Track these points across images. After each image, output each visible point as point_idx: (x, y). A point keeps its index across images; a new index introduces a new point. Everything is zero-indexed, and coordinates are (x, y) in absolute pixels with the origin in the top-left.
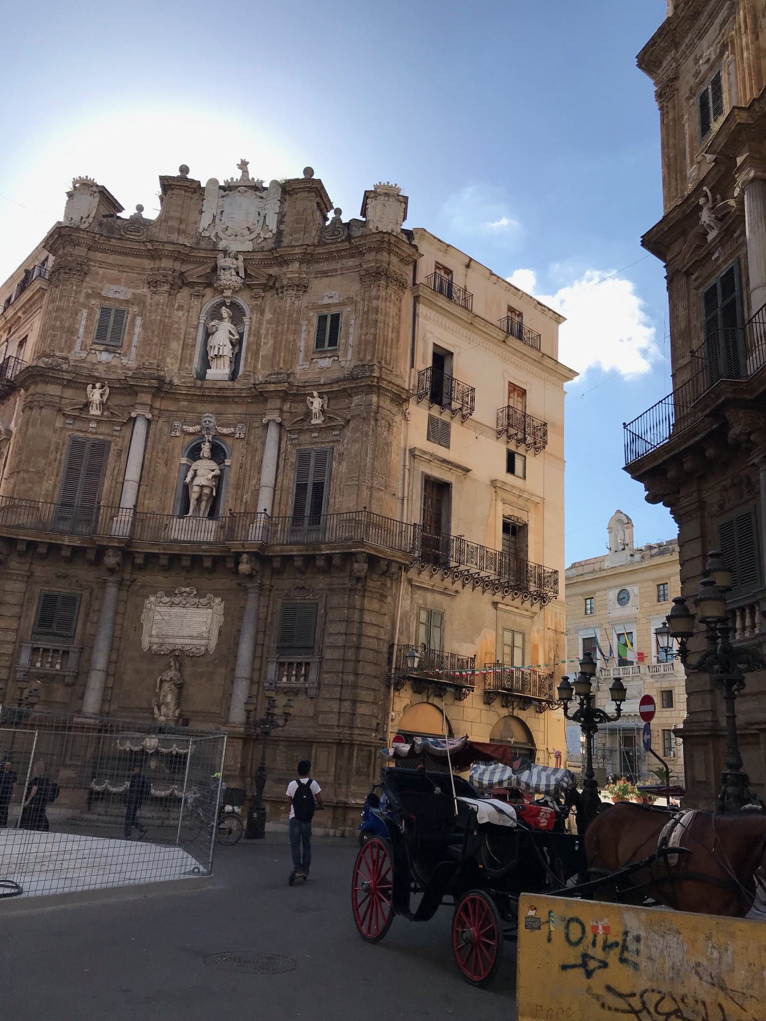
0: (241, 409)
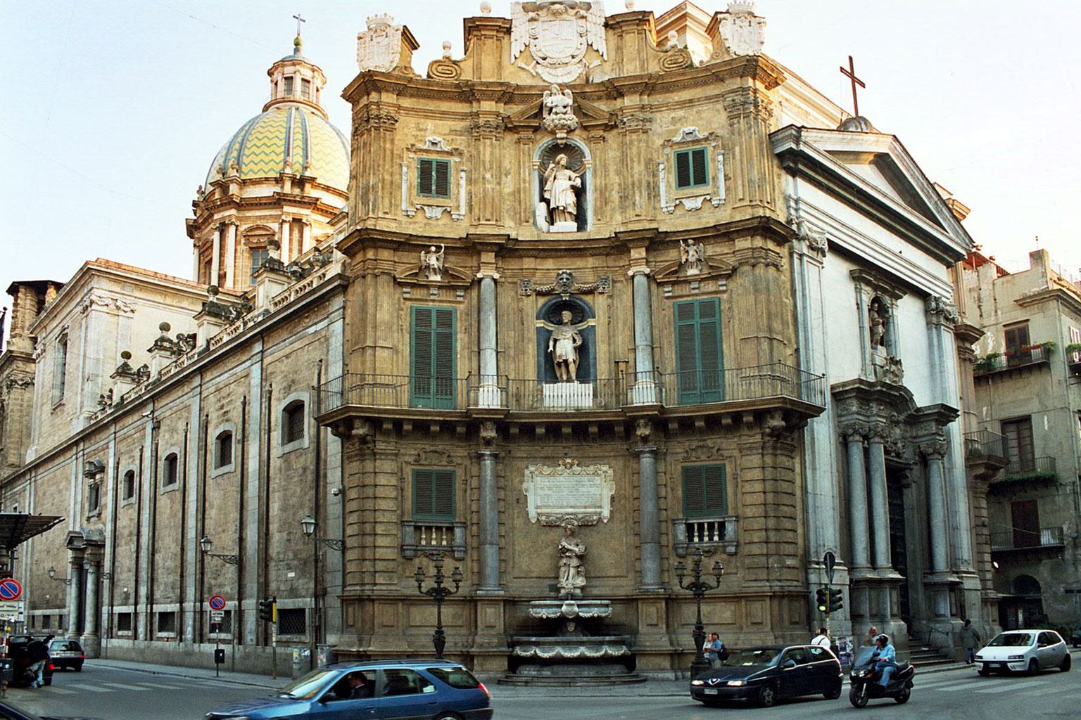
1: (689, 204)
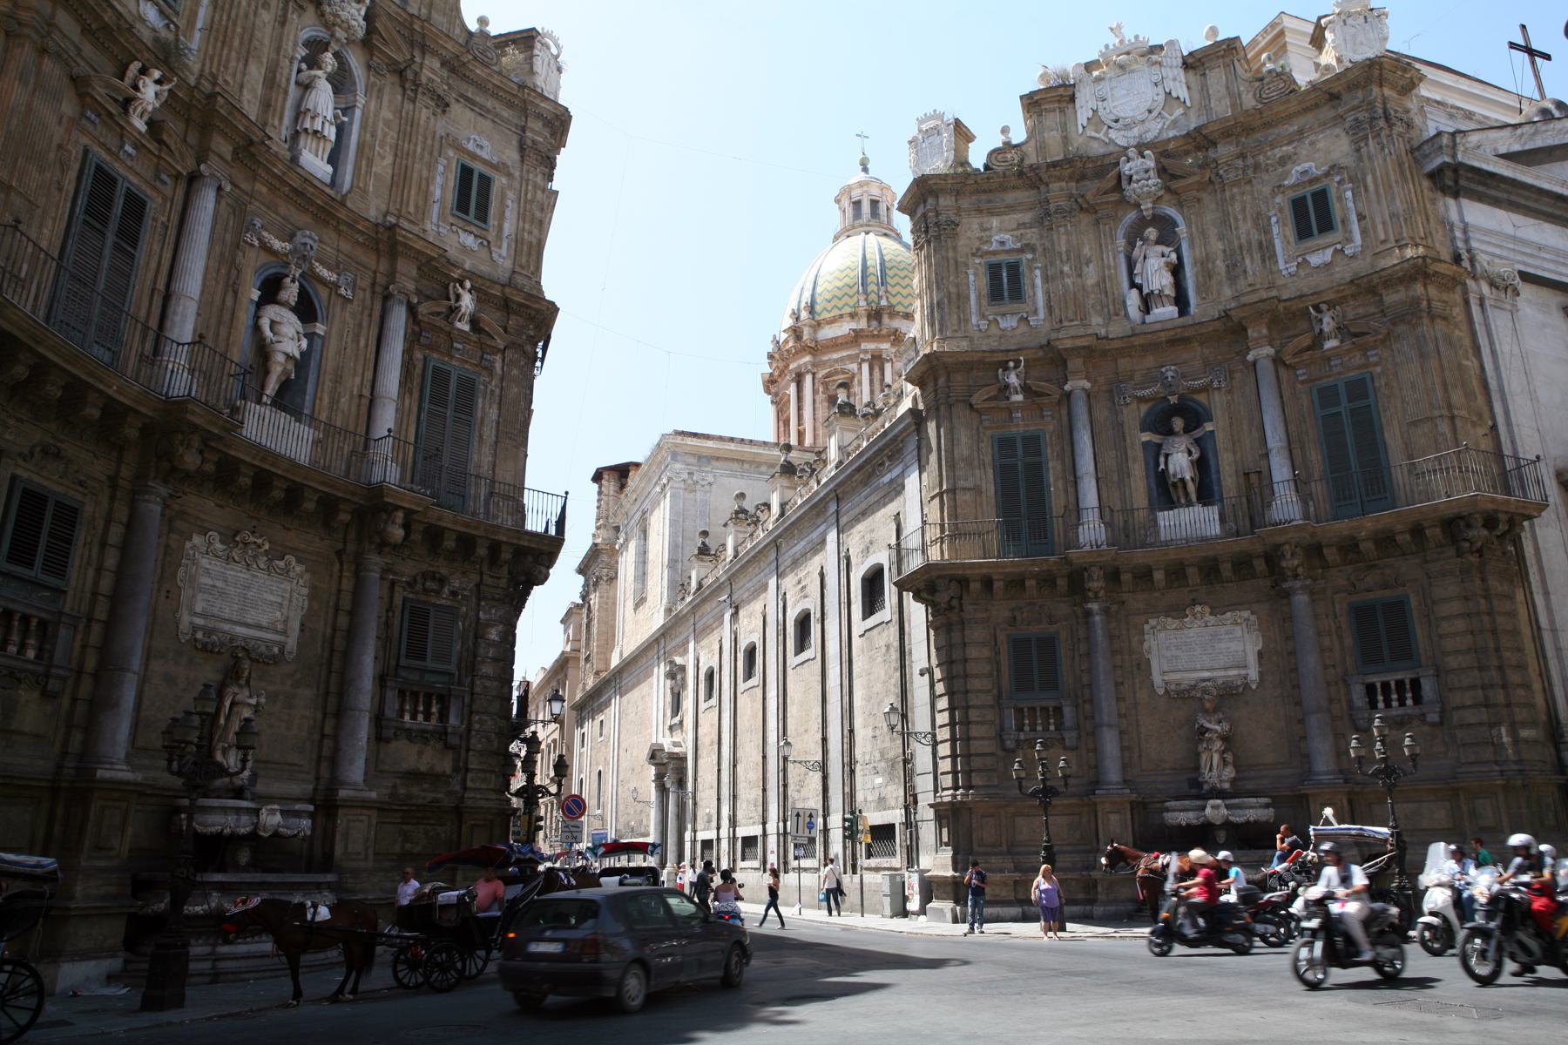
0: (345, 246)
1: (1315, 260)
